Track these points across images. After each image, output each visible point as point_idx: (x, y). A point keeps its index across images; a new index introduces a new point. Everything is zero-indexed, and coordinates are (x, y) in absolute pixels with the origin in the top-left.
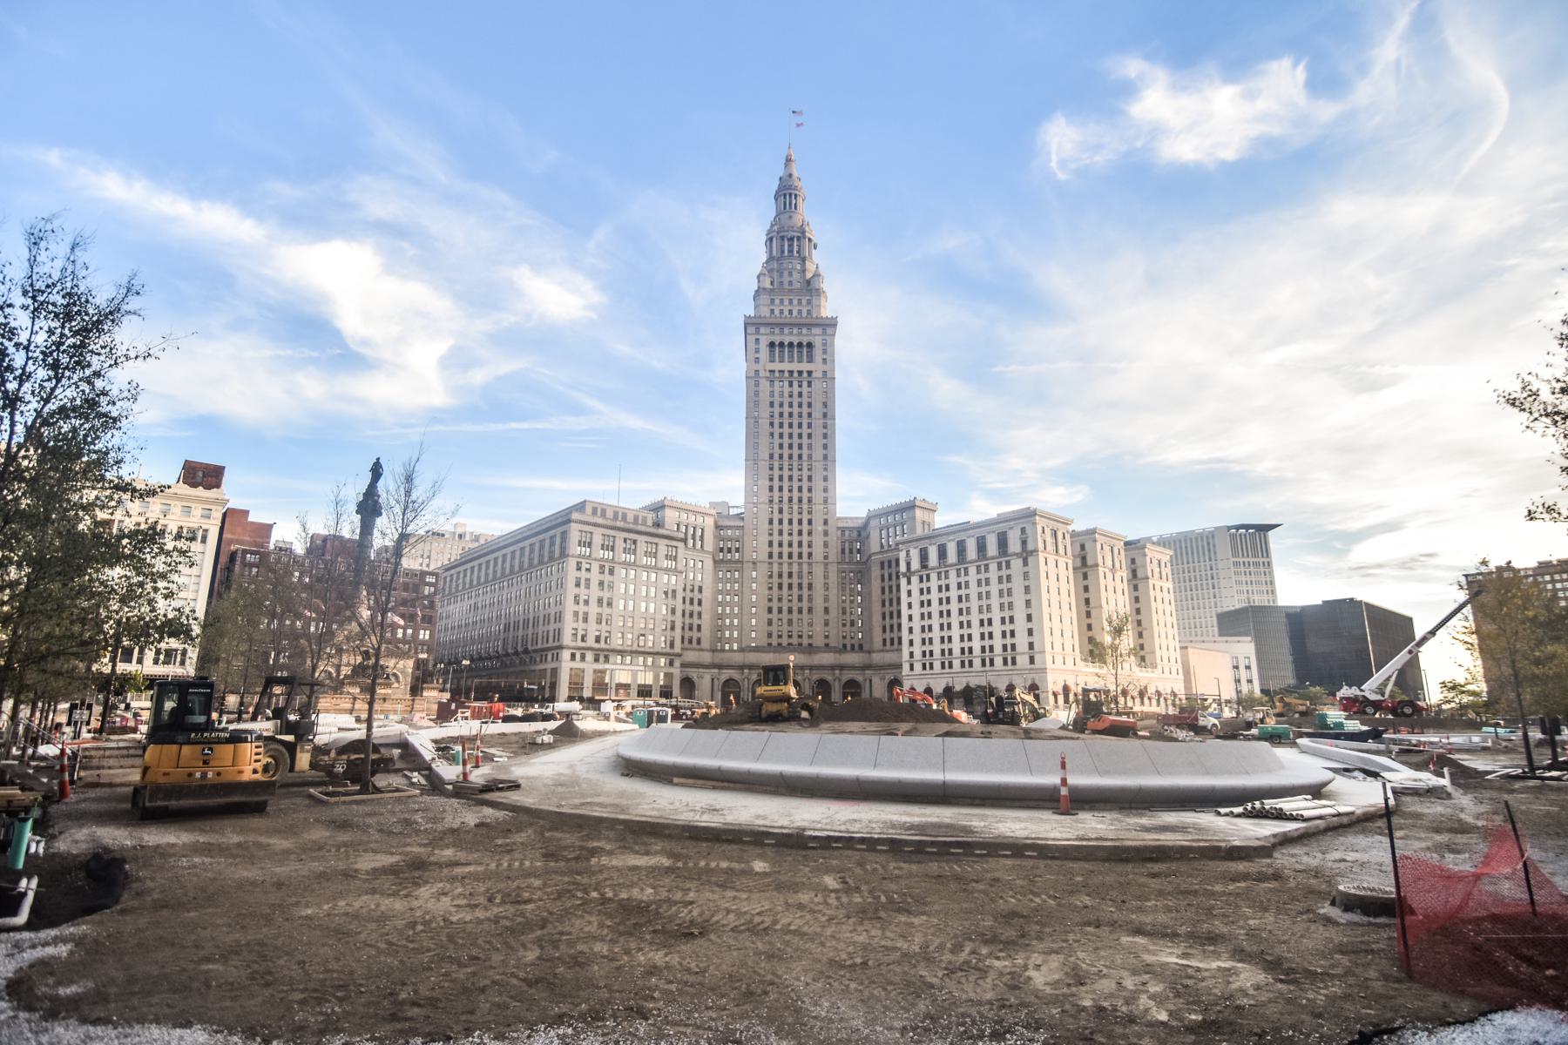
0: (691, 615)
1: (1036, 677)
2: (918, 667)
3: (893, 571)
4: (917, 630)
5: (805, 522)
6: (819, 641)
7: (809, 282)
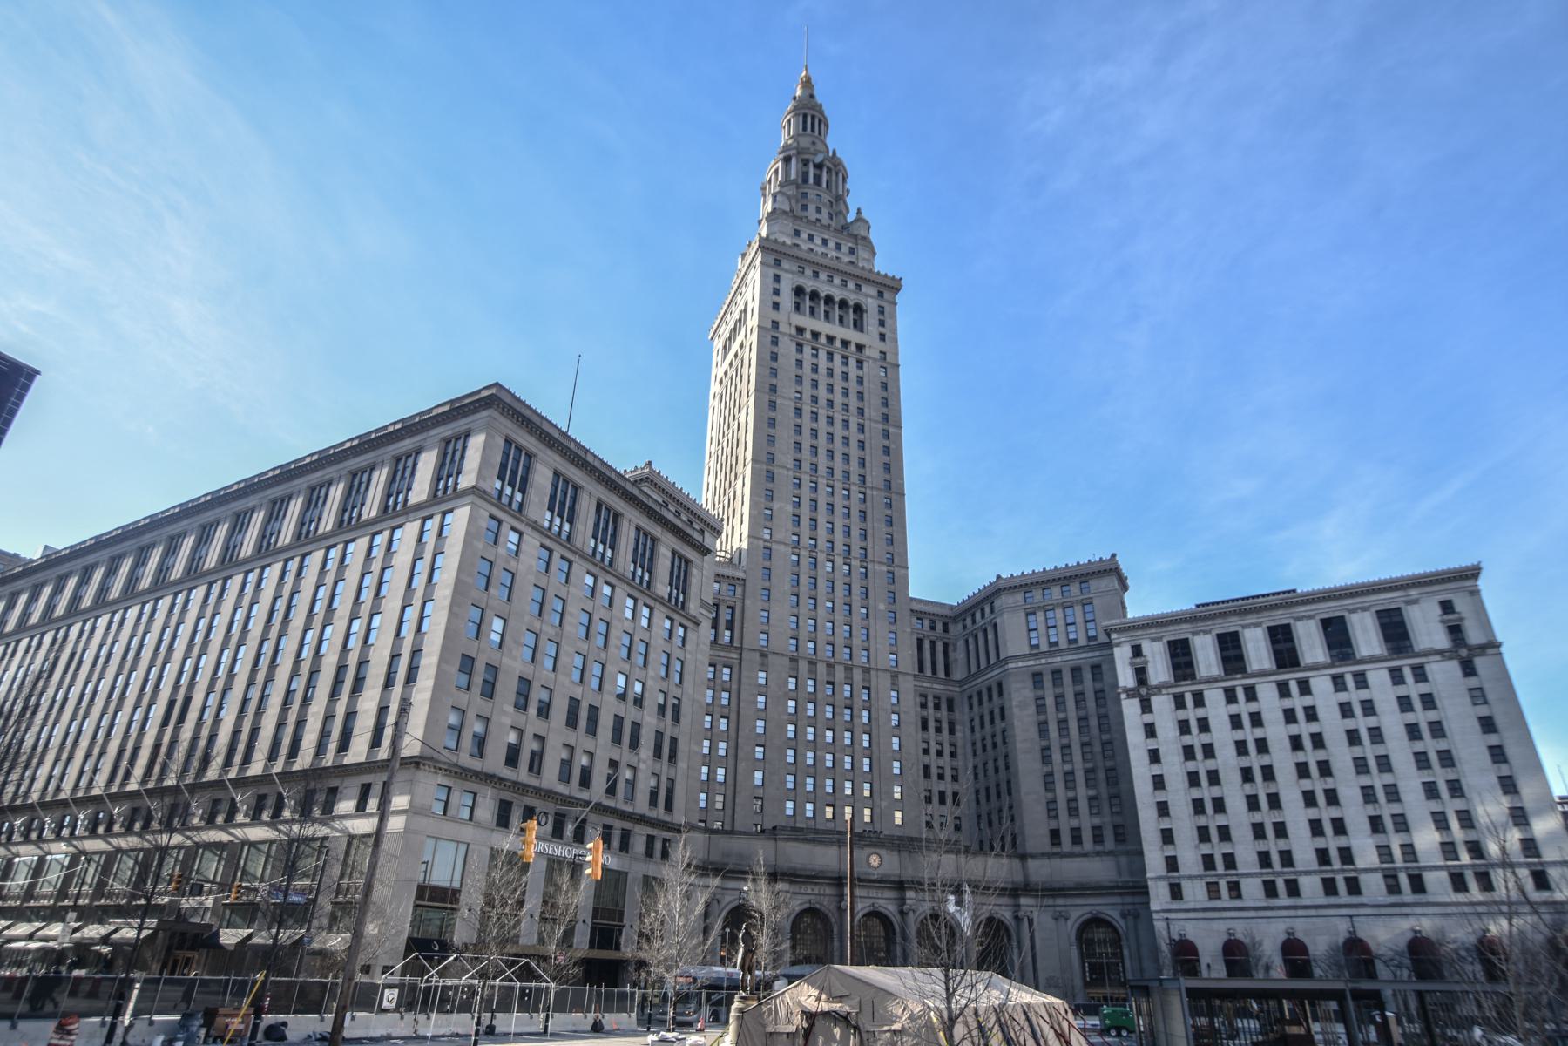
2: (1195, 893)
7: (846, 227)
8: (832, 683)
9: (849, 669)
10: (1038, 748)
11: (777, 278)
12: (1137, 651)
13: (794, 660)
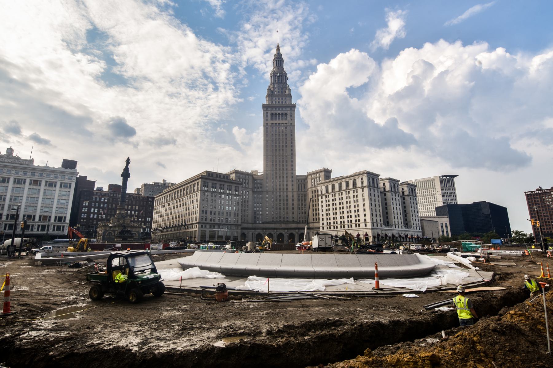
0: (245, 211)
1: (367, 231)
2: (325, 228)
3: (316, 194)
4: (325, 215)
5: (285, 177)
6: (290, 219)
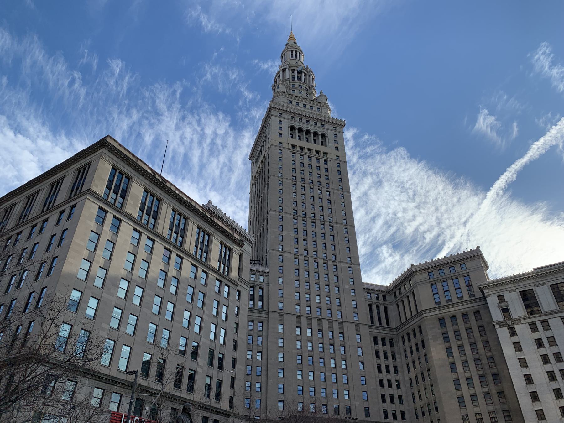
7: (316, 99)
8: (321, 331)
9: (330, 322)
10: (448, 364)
11: (280, 122)
12: (501, 298)
13: (299, 317)
